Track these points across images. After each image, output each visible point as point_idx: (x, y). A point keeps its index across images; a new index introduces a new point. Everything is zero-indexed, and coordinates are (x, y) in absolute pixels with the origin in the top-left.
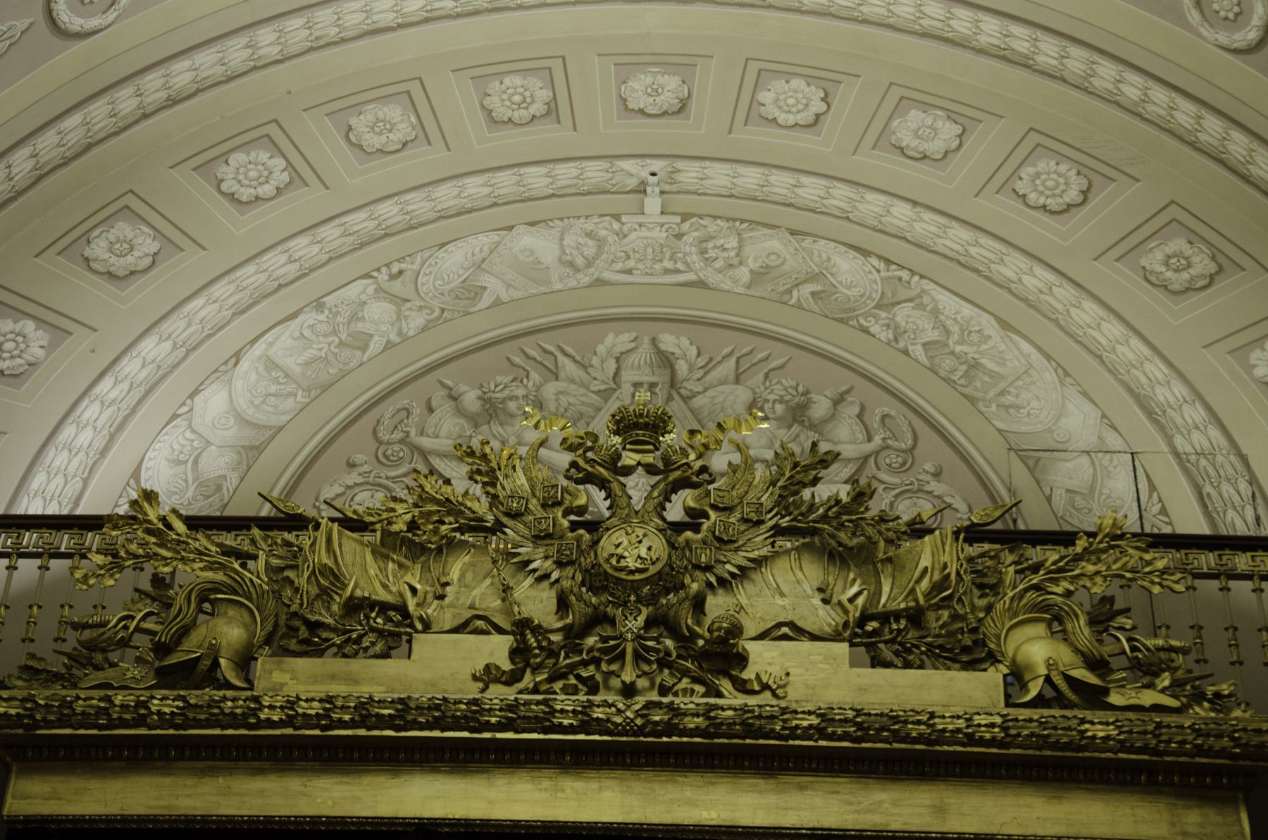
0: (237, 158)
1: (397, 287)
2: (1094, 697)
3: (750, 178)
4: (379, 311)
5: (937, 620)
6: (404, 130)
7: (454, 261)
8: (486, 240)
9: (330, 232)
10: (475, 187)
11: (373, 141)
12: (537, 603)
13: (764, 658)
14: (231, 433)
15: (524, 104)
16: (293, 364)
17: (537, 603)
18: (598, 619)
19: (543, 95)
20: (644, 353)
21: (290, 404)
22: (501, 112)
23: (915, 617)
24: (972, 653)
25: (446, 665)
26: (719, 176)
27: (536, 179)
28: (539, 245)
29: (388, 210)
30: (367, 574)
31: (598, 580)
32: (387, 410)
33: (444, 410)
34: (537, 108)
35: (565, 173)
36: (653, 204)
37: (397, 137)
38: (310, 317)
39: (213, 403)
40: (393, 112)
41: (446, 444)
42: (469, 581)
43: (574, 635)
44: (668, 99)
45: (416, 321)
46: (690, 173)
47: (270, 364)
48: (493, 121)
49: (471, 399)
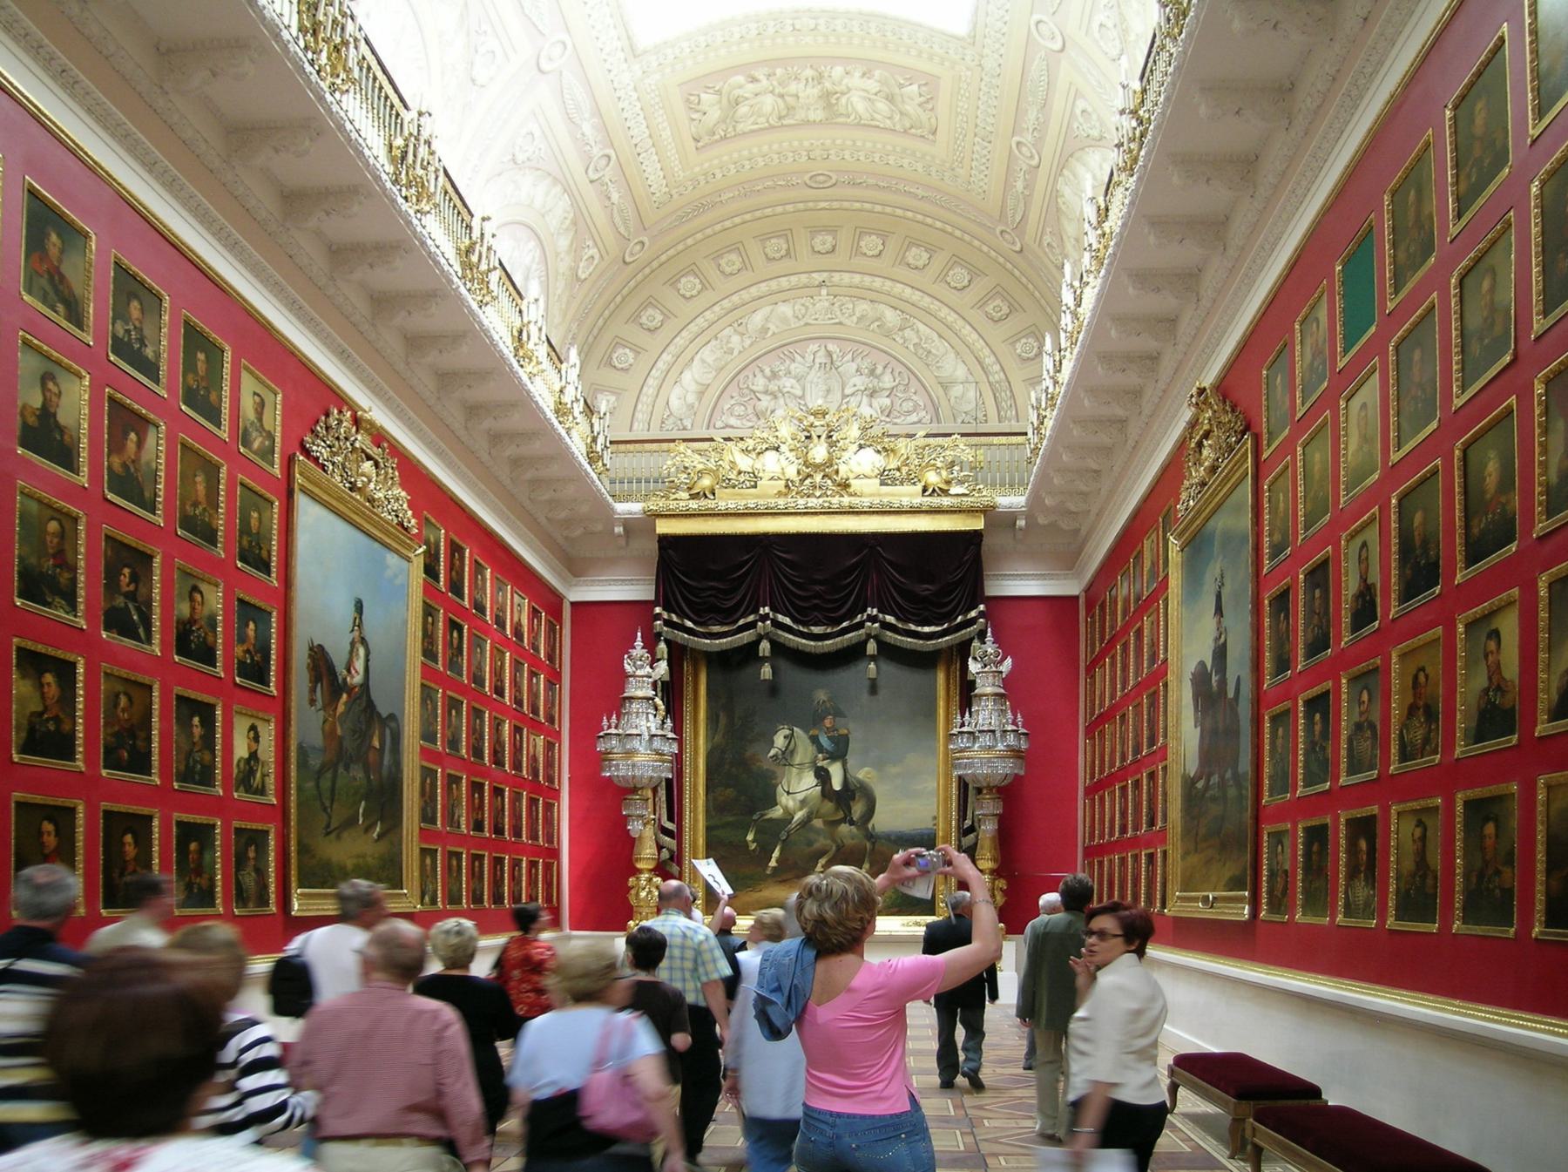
0: (684, 280)
1: (741, 329)
2: (945, 492)
3: (857, 278)
4: (736, 339)
5: (904, 470)
6: (738, 265)
7: (757, 319)
8: (768, 309)
9: (716, 308)
10: (764, 287)
11: (728, 270)
12: (791, 472)
13: (856, 485)
14: (693, 387)
15: (778, 251)
16: (710, 360)
17: (791, 472)
18: (809, 476)
19: (785, 246)
20: (822, 352)
21: (711, 376)
22: (771, 255)
23: (898, 469)
24: (911, 480)
25: (767, 492)
26: (846, 278)
27: (784, 282)
28: (785, 309)
29: (735, 298)
30: (745, 463)
31: (806, 464)
32: (741, 377)
33: (759, 375)
34: (783, 252)
35: (794, 279)
36: (824, 292)
37: (736, 267)
38: (713, 342)
39: (687, 377)
40: (734, 257)
41: (761, 388)
42: (771, 464)
43: (802, 481)
44: (828, 246)
45: (748, 342)
46: (836, 277)
47: (703, 361)
48: (769, 259)
49: (767, 372)
